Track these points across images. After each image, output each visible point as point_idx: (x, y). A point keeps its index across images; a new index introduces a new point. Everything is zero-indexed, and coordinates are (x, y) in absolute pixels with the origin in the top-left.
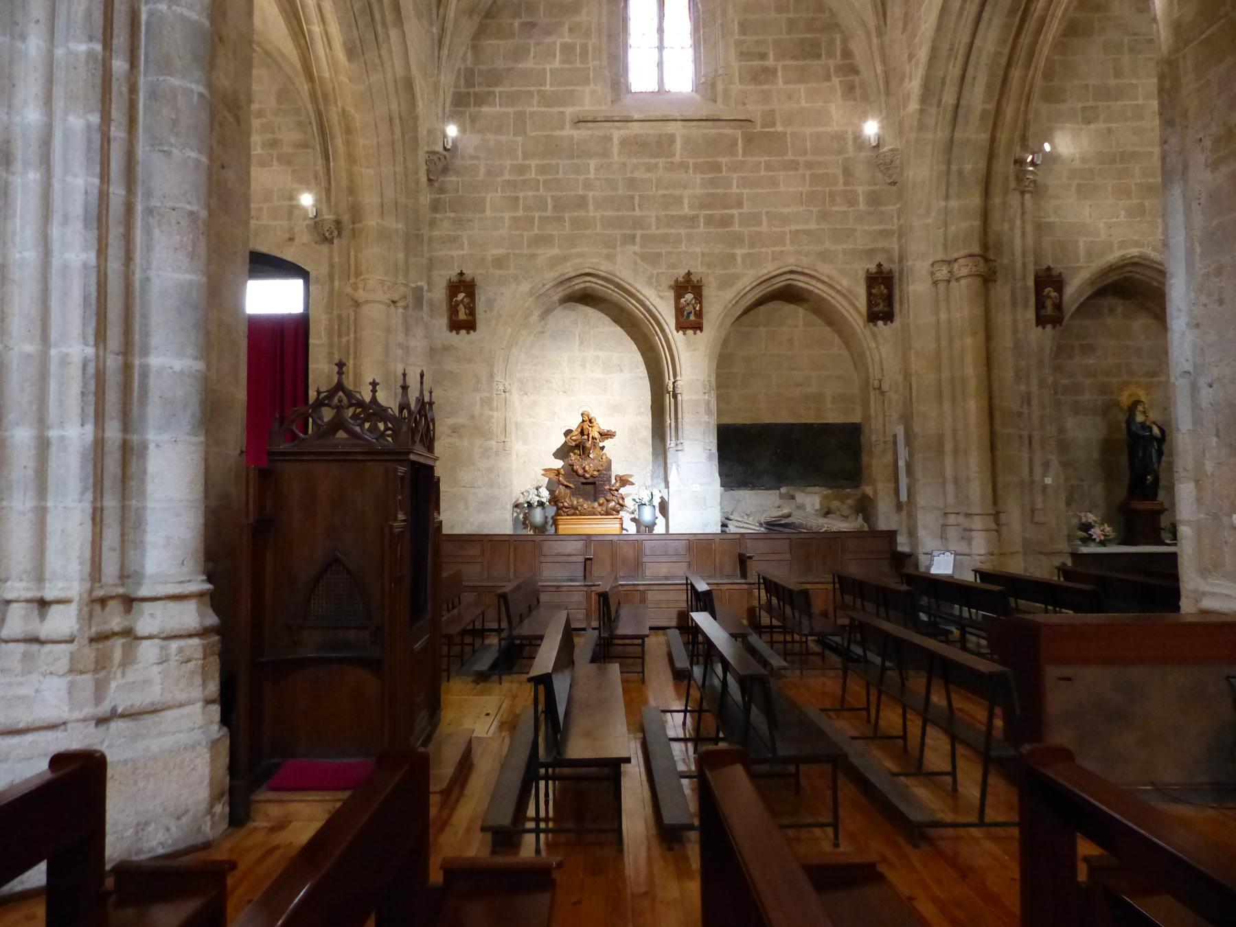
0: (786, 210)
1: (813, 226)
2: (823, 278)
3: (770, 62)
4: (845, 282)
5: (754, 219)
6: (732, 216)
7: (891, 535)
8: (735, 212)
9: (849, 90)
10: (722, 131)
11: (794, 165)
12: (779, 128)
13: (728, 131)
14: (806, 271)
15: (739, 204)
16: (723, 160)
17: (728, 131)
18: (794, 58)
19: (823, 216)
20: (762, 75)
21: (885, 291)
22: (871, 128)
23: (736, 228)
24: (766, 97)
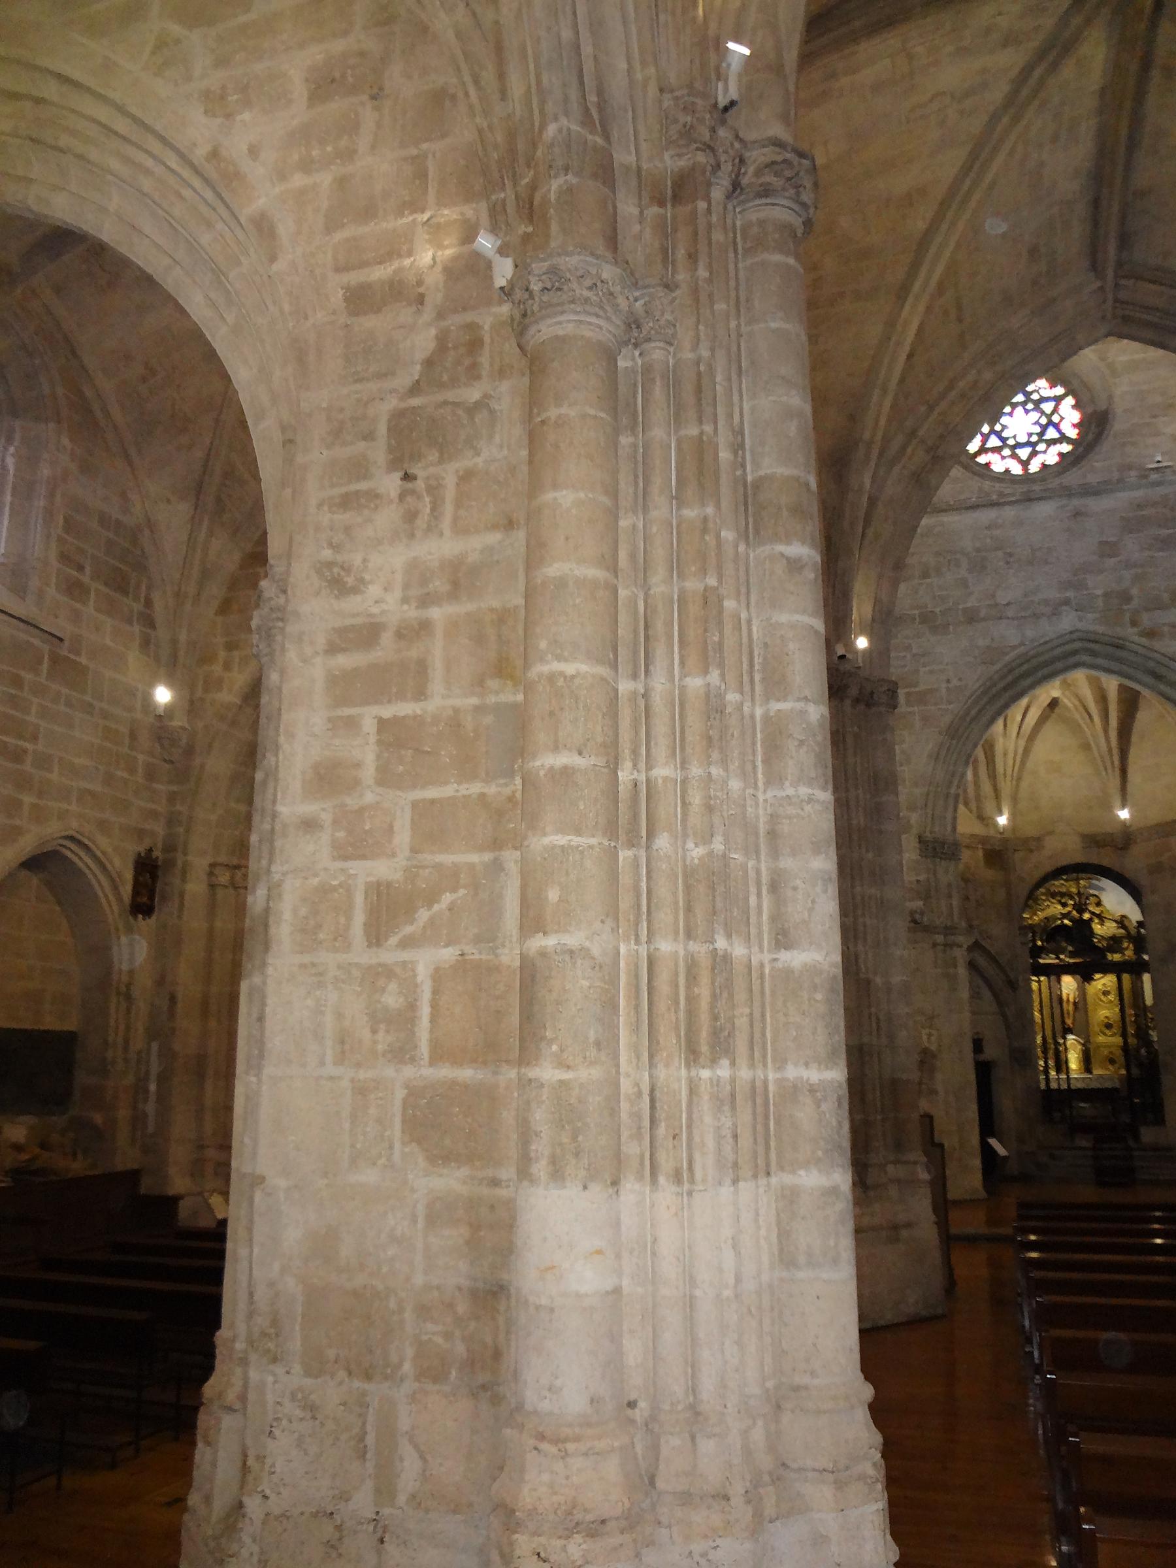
0: (77, 761)
1: (97, 787)
2: (99, 854)
3: (86, 579)
4: (117, 862)
5: (44, 762)
6: (25, 751)
7: (133, 1176)
8: (27, 745)
9: (146, 643)
10: (31, 640)
11: (88, 709)
12: (83, 660)
13: (36, 642)
14: (86, 842)
15: (35, 738)
16: (28, 676)
17: (36, 642)
18: (106, 584)
19: (109, 780)
20: (75, 589)
21: (150, 881)
22: (163, 695)
23: (28, 767)
24: (76, 617)
